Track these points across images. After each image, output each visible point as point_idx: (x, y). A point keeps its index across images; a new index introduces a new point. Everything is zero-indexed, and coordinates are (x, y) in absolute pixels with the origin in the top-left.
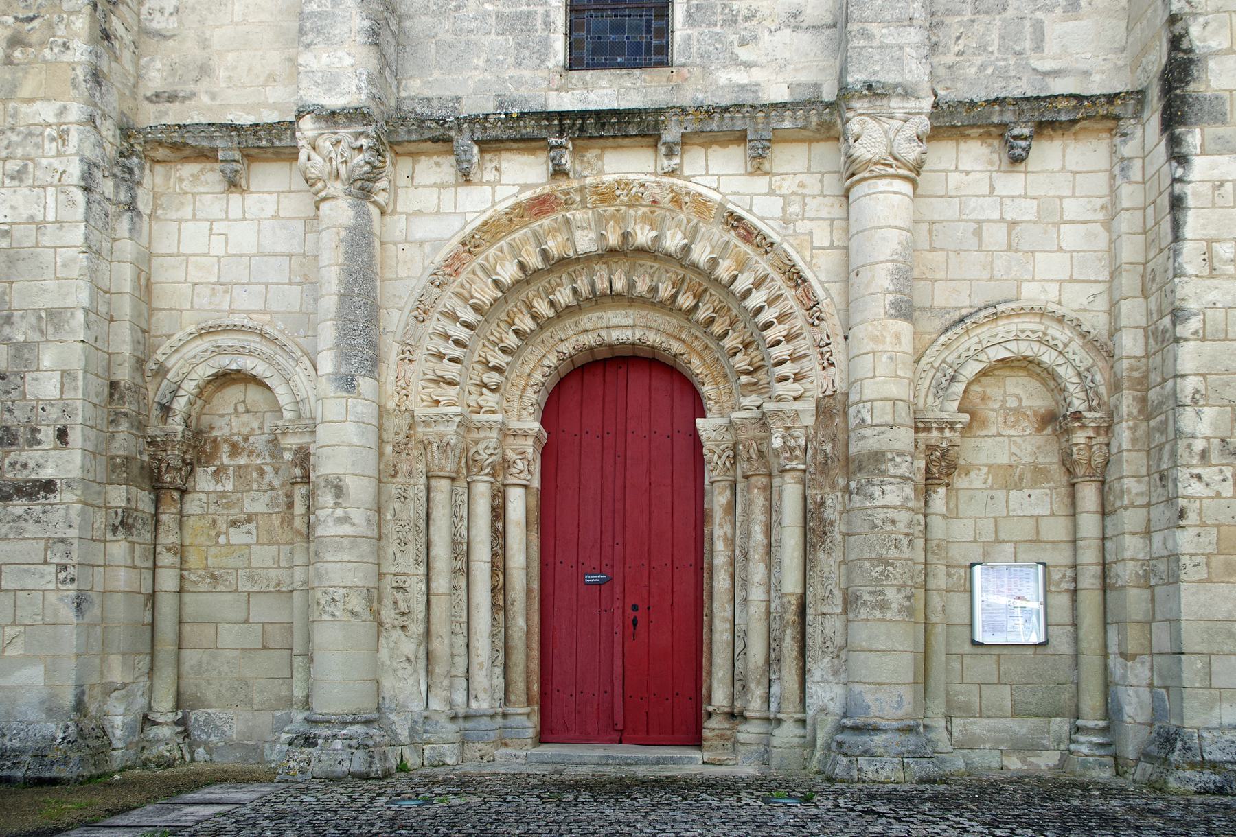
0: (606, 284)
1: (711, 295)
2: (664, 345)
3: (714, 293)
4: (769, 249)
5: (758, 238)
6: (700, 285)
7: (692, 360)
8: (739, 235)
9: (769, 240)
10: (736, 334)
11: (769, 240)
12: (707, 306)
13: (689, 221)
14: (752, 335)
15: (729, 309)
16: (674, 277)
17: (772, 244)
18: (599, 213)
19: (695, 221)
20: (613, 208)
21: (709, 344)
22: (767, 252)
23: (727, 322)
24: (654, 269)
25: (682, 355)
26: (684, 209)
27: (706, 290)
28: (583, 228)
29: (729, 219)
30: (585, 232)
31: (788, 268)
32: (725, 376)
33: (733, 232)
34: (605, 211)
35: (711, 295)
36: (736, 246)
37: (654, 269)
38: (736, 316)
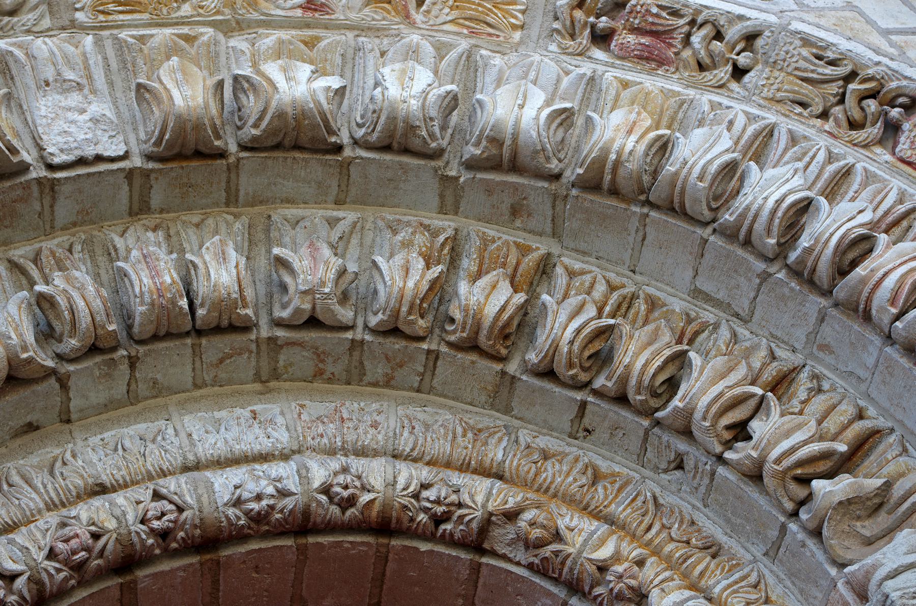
0: (169, 276)
1: (572, 274)
2: (431, 494)
3: (577, 266)
4: (743, 60)
5: (696, 39)
6: (524, 250)
7: (561, 524)
8: (625, 55)
9: (733, 33)
10: (719, 362)
11: (733, 33)
12: (573, 301)
13: (441, 50)
14: (773, 357)
15: (653, 304)
16: (421, 239)
17: (750, 38)
18: (120, 45)
19: (464, 45)
20: (168, 31)
21: (604, 466)
22: (739, 73)
23: (666, 337)
24: (342, 227)
25: (511, 516)
26: (418, 17)
27: (545, 268)
28: (65, 87)
29: (579, 14)
30: (75, 99)
31: (834, 88)
32: (713, 549)
33: (598, 54)
34: (142, 39)
35: (572, 274)
36: (625, 85)
37: (342, 227)
38: (689, 321)
